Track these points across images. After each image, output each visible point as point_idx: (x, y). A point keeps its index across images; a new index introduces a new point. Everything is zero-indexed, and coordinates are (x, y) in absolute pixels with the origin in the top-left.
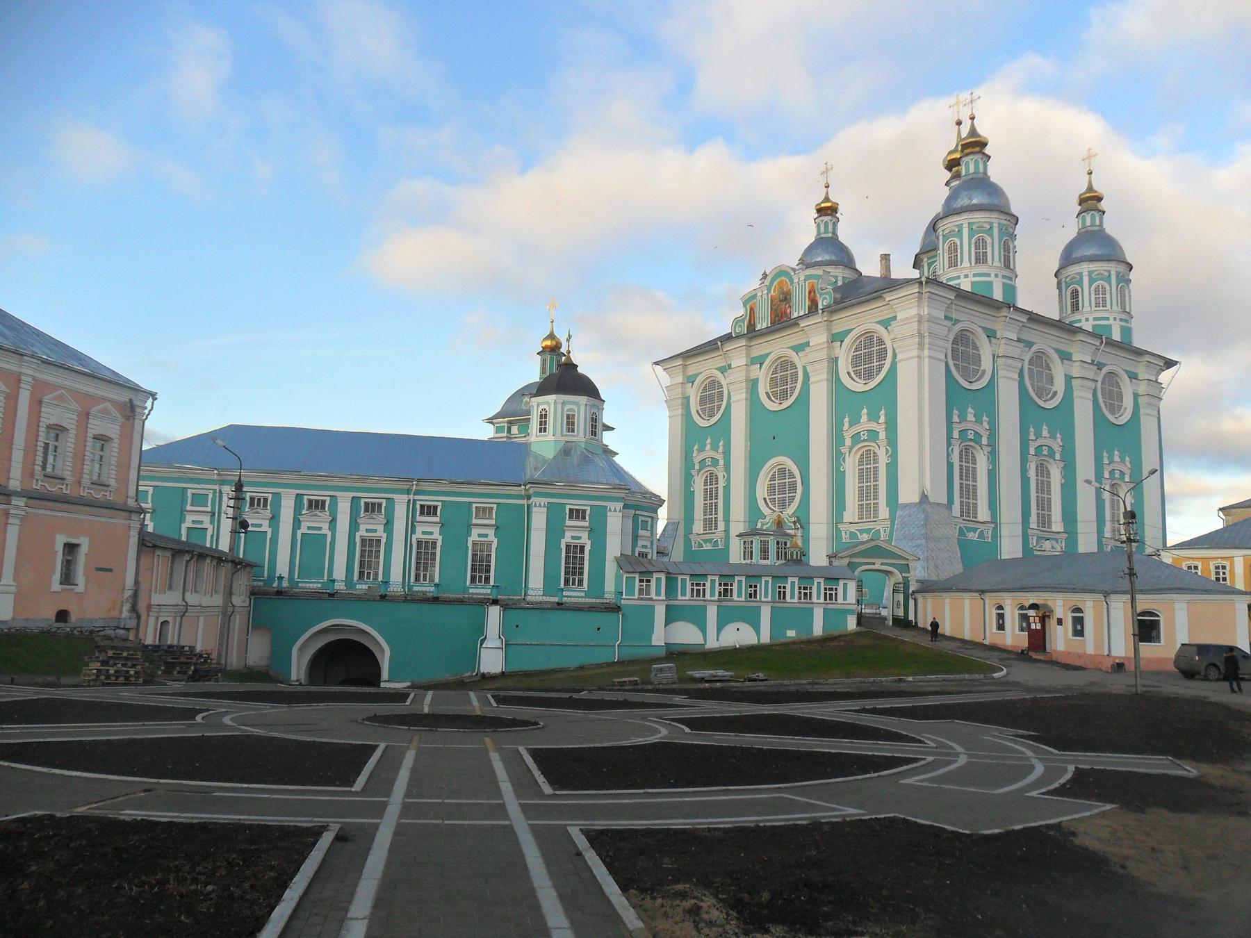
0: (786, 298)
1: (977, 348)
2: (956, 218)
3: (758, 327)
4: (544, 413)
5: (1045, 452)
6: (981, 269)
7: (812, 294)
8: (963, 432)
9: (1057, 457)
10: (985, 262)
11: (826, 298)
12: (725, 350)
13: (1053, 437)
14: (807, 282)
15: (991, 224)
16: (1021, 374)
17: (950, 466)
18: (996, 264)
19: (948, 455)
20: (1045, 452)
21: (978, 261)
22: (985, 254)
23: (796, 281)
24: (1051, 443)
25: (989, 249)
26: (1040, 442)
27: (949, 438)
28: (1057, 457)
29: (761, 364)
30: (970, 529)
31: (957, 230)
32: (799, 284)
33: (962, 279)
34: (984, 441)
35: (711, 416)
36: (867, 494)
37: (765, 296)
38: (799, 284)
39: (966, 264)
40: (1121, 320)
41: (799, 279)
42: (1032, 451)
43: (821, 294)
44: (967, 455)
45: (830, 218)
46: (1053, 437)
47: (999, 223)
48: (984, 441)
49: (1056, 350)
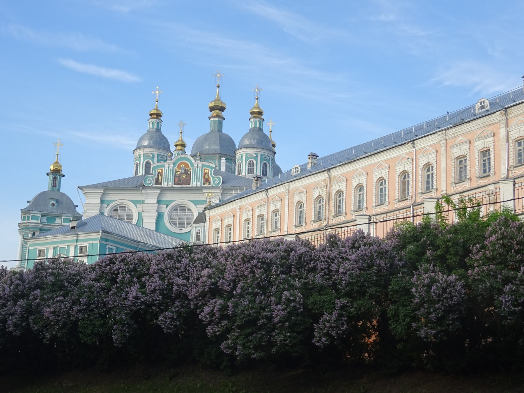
0: (187, 172)
2: (255, 150)
3: (165, 184)
4: (198, 231)
7: (206, 175)
11: (217, 180)
12: (143, 192)
14: (204, 168)
15: (257, 154)
23: (195, 165)
25: (268, 169)
29: (167, 206)
31: (255, 156)
32: (198, 168)
37: (171, 168)
38: (198, 168)
41: (198, 165)
43: (213, 177)
45: (155, 120)
47: (261, 154)
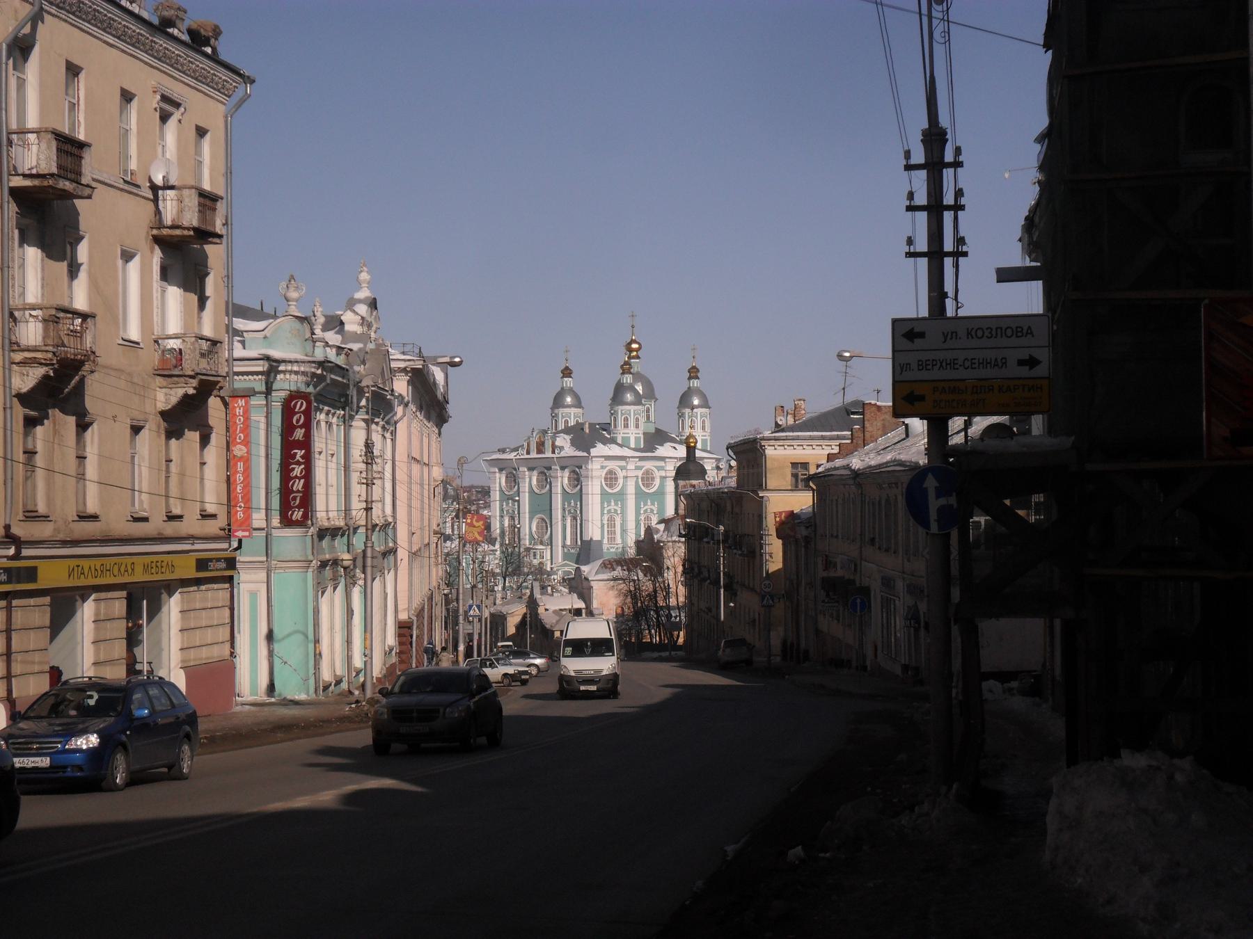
1: (615, 474)
5: (649, 511)
6: (626, 431)
8: (609, 511)
9: (655, 512)
10: (627, 427)
13: (654, 505)
16: (637, 482)
17: (603, 526)
18: (632, 428)
19: (602, 520)
20: (649, 511)
21: (624, 427)
22: (627, 424)
24: (652, 507)
26: (645, 508)
27: (602, 514)
28: (655, 512)
30: (611, 548)
33: (618, 435)
34: (619, 512)
35: (511, 489)
36: (574, 534)
39: (619, 428)
40: (702, 436)
42: (642, 512)
44: (611, 520)
46: (654, 505)
48: (619, 512)
49: (655, 467)
